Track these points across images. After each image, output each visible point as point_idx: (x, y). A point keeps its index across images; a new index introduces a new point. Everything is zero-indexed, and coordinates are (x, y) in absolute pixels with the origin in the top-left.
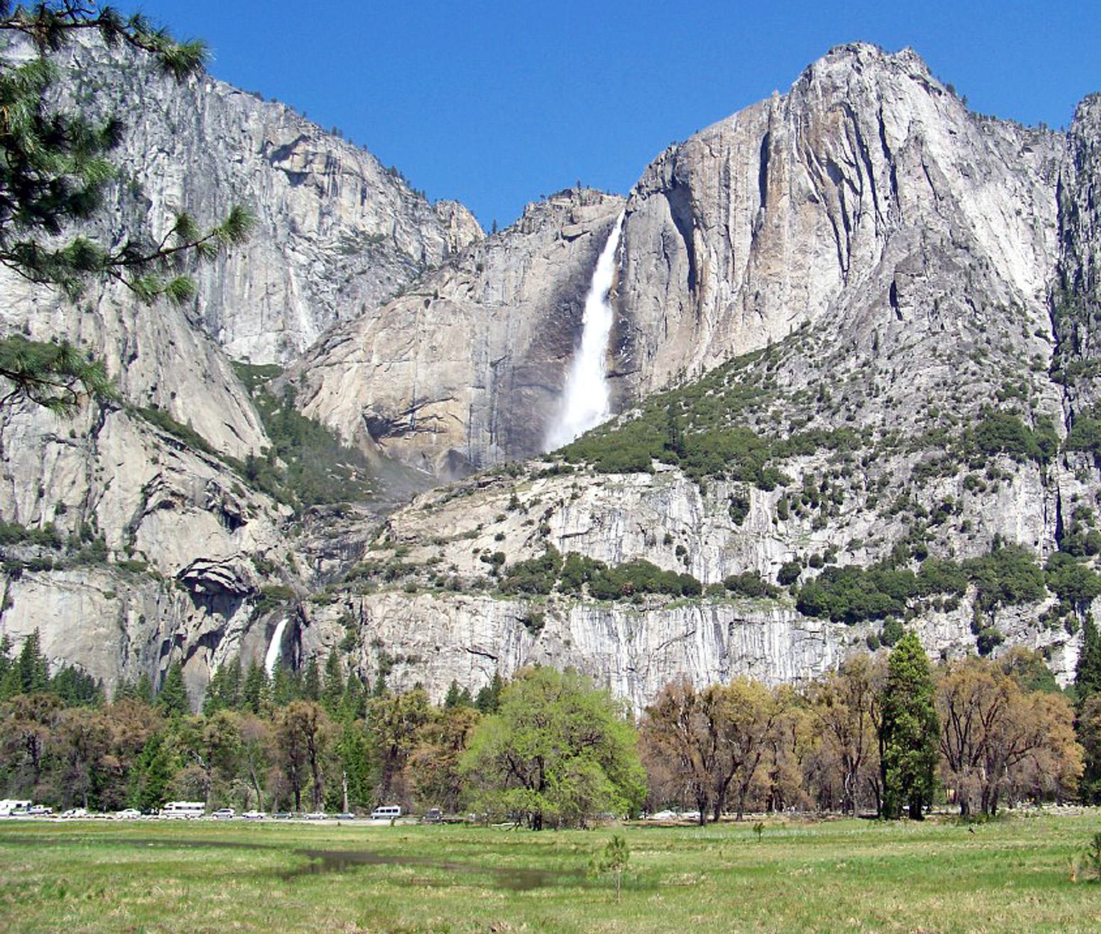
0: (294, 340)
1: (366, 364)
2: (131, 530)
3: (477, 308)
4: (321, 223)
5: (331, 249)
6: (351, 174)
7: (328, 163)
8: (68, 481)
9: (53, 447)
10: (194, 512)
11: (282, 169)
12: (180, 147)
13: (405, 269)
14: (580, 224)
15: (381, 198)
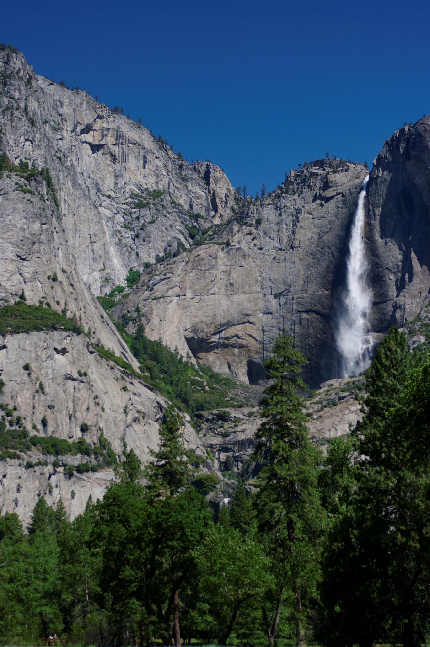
0: (112, 277)
1: (183, 297)
2: (123, 439)
3: (260, 253)
4: (116, 184)
5: (126, 204)
6: (134, 144)
7: (117, 136)
8: (84, 408)
9: (70, 383)
10: (149, 424)
11: (86, 143)
12: (38, 136)
13: (180, 217)
14: (335, 188)
15: (157, 162)
